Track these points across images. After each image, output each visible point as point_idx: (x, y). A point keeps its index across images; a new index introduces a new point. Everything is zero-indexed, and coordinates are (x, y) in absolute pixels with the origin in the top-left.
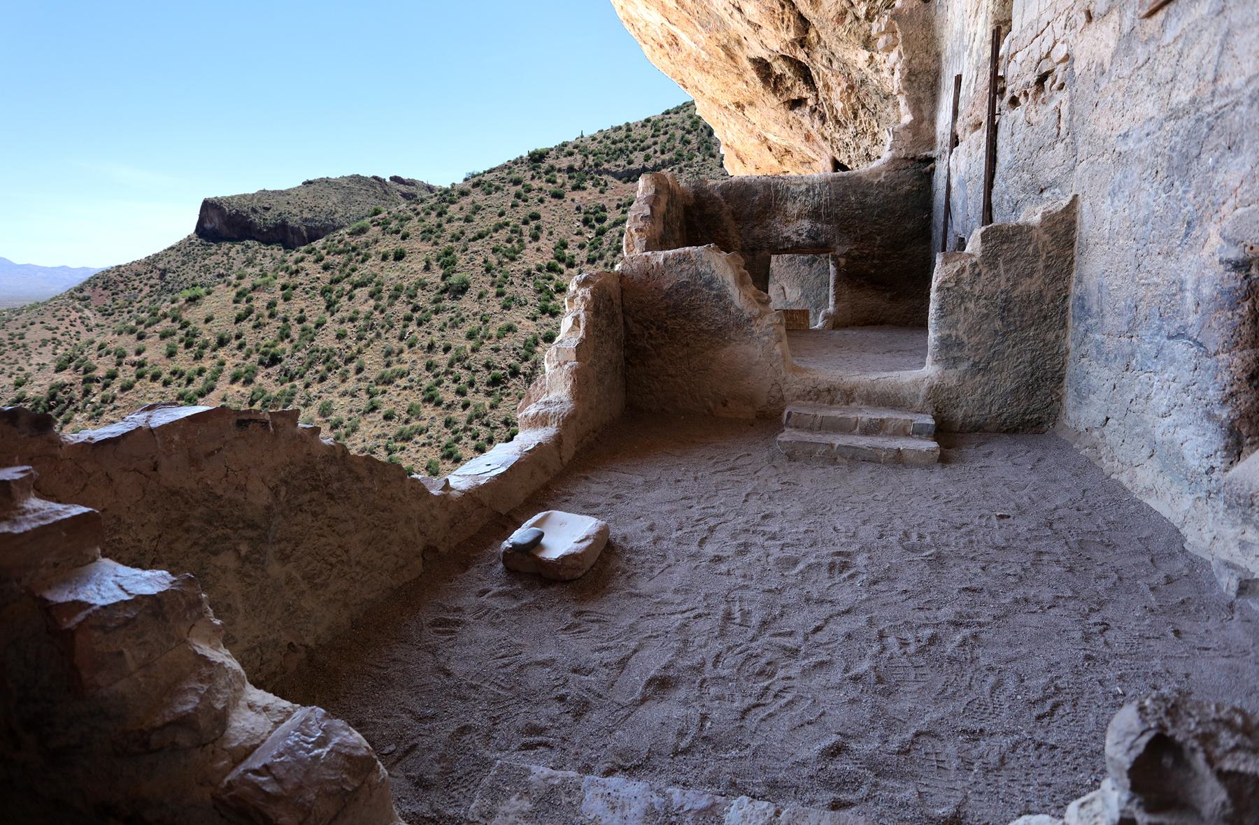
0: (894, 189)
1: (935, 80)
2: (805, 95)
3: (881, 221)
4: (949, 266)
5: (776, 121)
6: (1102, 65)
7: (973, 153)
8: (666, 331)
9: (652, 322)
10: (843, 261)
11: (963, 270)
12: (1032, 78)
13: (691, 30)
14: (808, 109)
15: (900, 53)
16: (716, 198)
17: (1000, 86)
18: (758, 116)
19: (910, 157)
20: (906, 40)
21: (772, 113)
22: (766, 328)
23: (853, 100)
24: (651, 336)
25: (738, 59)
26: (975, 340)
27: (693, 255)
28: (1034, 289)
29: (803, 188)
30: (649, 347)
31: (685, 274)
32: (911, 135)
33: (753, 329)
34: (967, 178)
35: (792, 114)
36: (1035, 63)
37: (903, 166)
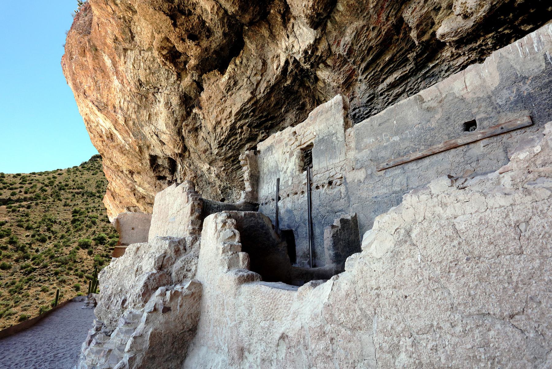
2: (167, 175)
4: (333, 229)
5: (149, 183)
6: (360, 180)
11: (337, 231)
14: (167, 181)
18: (140, 179)
20: (250, 164)
21: (149, 179)
23: (195, 182)
25: (143, 154)
26: (343, 254)
27: (256, 214)
28: (353, 238)
29: (216, 206)
31: (253, 222)
34: (293, 209)
35: (158, 182)
36: (327, 178)
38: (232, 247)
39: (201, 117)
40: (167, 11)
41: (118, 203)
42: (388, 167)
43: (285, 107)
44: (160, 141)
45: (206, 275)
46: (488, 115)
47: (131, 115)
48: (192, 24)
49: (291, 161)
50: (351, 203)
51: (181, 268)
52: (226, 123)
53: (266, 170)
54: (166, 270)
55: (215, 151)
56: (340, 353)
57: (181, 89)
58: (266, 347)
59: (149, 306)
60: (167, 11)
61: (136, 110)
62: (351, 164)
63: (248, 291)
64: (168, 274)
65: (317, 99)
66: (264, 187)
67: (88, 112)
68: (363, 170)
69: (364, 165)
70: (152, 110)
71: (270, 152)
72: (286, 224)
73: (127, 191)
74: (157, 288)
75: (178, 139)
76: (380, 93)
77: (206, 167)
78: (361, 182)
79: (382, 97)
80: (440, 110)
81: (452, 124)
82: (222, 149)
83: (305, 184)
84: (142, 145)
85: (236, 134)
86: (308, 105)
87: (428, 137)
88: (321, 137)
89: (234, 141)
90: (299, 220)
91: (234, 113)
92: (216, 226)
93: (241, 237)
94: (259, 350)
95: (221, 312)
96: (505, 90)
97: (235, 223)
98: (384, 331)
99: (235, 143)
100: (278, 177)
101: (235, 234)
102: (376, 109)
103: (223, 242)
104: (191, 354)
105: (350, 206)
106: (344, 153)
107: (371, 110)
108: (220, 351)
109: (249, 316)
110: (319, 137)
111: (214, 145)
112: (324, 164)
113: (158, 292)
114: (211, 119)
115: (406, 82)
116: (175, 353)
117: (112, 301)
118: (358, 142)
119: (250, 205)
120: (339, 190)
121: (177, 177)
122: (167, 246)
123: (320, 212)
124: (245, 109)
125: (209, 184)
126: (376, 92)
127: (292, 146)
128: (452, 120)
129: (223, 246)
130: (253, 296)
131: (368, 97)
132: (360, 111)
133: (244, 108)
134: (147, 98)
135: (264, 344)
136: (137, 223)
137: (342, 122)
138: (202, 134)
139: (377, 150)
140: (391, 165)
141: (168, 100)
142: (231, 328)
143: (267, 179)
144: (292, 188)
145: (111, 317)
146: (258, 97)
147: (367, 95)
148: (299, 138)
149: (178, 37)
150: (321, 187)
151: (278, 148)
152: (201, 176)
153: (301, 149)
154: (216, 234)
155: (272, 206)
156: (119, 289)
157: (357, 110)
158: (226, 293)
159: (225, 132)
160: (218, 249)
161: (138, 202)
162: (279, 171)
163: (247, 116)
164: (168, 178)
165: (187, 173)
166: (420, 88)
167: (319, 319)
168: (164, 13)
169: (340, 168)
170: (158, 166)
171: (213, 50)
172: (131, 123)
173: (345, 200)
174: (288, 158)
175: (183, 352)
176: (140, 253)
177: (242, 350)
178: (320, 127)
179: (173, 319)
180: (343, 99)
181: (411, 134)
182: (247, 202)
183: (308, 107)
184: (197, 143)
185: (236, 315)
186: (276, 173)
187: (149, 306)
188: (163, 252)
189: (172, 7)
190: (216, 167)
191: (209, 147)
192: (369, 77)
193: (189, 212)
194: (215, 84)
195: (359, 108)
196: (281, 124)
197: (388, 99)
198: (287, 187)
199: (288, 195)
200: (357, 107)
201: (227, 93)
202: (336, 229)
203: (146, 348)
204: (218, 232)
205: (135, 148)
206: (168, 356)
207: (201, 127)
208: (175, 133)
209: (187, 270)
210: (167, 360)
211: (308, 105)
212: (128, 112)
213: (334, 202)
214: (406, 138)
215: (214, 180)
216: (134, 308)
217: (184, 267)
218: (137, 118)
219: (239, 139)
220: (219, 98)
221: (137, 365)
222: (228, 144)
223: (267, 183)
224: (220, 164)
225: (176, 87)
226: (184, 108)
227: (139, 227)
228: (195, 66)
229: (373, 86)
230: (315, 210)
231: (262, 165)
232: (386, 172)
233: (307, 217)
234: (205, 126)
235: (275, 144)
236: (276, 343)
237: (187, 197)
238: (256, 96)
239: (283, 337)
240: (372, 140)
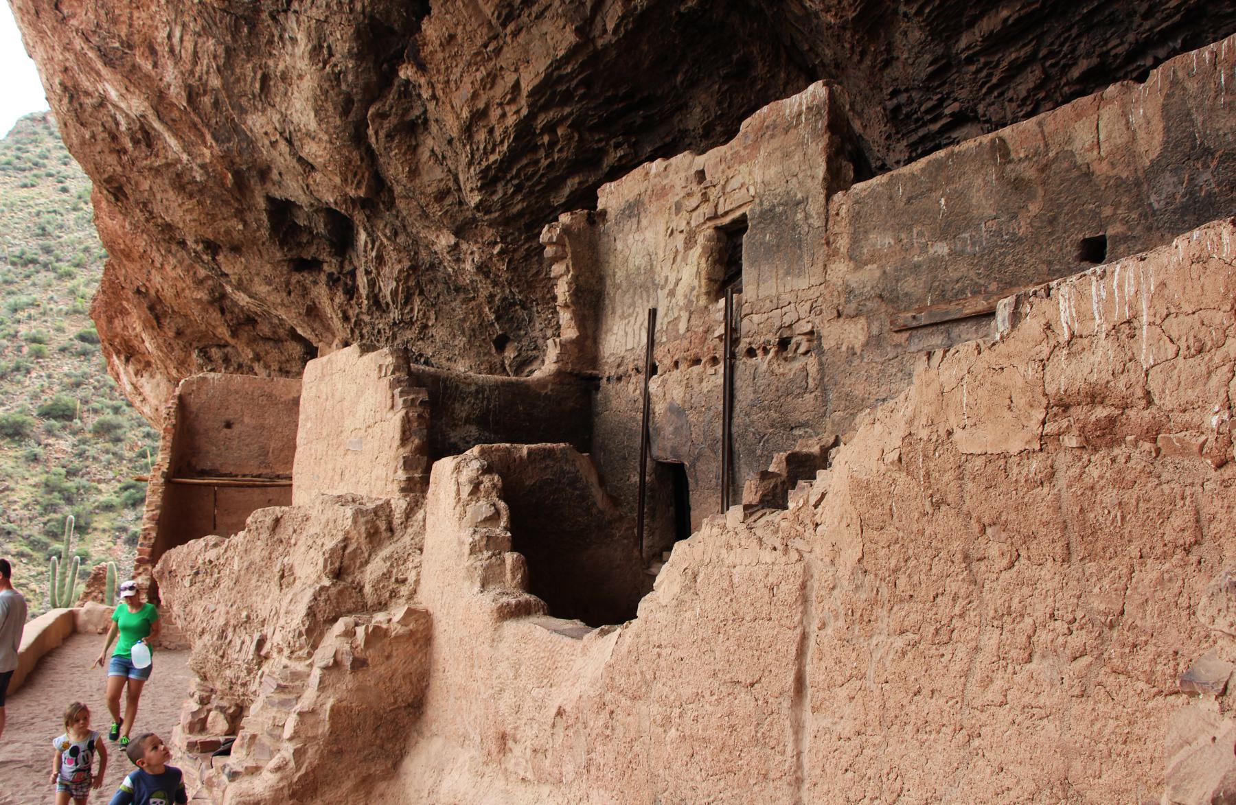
1: (598, 301)
2: (324, 256)
4: (765, 483)
6: (853, 348)
7: (696, 385)
11: (776, 486)
12: (774, 339)
14: (323, 278)
15: (567, 267)
17: (734, 336)
21: (268, 270)
22: (626, 530)
23: (412, 283)
29: (473, 388)
31: (549, 470)
32: (576, 350)
33: (613, 531)
34: (687, 406)
35: (296, 277)
36: (775, 328)
38: (491, 542)
39: (426, 94)
41: (171, 334)
42: (914, 324)
43: (687, 71)
44: (300, 160)
45: (439, 596)
46: (1129, 229)
47: (205, 77)
49: (689, 261)
50: (831, 407)
51: (384, 574)
52: (504, 115)
53: (620, 275)
54: (350, 580)
55: (474, 199)
56: (620, 731)
58: (539, 730)
59: (324, 655)
61: (221, 61)
62: (836, 301)
63: (515, 635)
64: (355, 588)
66: (615, 328)
67: (71, 63)
68: (863, 320)
69: (865, 309)
70: (271, 63)
71: (635, 220)
72: (668, 444)
74: (335, 620)
75: (356, 156)
76: (963, 56)
77: (445, 240)
78: (854, 354)
79: (973, 68)
80: (1041, 192)
81: (1058, 238)
83: (720, 337)
84: (244, 167)
85: (536, 148)
86: (760, 64)
87: (1009, 259)
88: (766, 205)
90: (701, 438)
91: (526, 87)
92: (458, 490)
93: (513, 519)
94: (528, 735)
95: (468, 670)
96: (1168, 174)
97: (500, 484)
98: (663, 700)
99: (535, 173)
100: (650, 306)
101: (497, 512)
102: (955, 100)
103: (471, 530)
104: (413, 752)
105: (828, 415)
106: (821, 265)
107: (941, 102)
108: (467, 742)
109: (516, 679)
110: (761, 203)
111: (469, 180)
112: (770, 288)
113: (340, 626)
114: (457, 103)
115: (1039, 31)
116: (382, 747)
117: (231, 641)
118: (855, 241)
120: (804, 369)
121: (356, 263)
122: (350, 522)
123: (753, 422)
124: (561, 78)
125: (457, 290)
126: (954, 51)
127: (695, 214)
128: (1061, 225)
129: (471, 540)
130: (523, 645)
131: (930, 65)
132: (910, 101)
133: (555, 74)
134: (253, 27)
135: (536, 726)
136: (239, 407)
137: (821, 171)
138: (430, 142)
139: (896, 270)
140: (923, 322)
141: (320, 38)
142: (485, 700)
143: (623, 303)
144: (685, 343)
145: (232, 676)
146: (600, 43)
147: (928, 57)
148: (713, 193)
150: (760, 352)
151: (656, 214)
152: (432, 266)
153: (717, 228)
154: (458, 508)
155: (632, 389)
156: (244, 614)
157: (903, 98)
158: (478, 635)
159: (502, 142)
160: (461, 543)
161: (234, 334)
162: (657, 287)
163: (567, 98)
164: (325, 267)
165: (386, 258)
166: (1077, 53)
167: (598, 685)
169: (807, 306)
170: (295, 229)
172: (207, 100)
173: (816, 398)
174: (681, 247)
175: (397, 747)
176: (285, 532)
177: (503, 737)
178: (767, 173)
179: (372, 682)
180: (831, 96)
181: (974, 244)
182: (565, 373)
183: (760, 69)
184: (414, 173)
185: (494, 677)
186: (647, 289)
187: (324, 655)
188: (340, 537)
190: (476, 242)
191: (451, 184)
192: (927, 11)
193: (398, 436)
195: (907, 90)
196: (676, 120)
197: (990, 76)
198: (676, 338)
199: (676, 365)
200: (903, 88)
201: (504, 25)
202: (773, 482)
203: (323, 735)
204: (461, 504)
206: (366, 752)
207: (426, 121)
209: (397, 580)
210: (365, 760)
211: (760, 64)
212: (198, 68)
213: (789, 399)
214: (961, 253)
215: (472, 281)
216: (290, 658)
217: (390, 572)
218: (226, 86)
219: (544, 163)
220: (479, 42)
221: (311, 763)
222: (512, 178)
223: (623, 317)
224: (489, 234)
226: (371, 65)
227: (246, 420)
229: (945, 35)
230: (741, 415)
231: (612, 259)
232: (911, 335)
233: (719, 433)
234: (437, 121)
235: (646, 200)
236: (550, 723)
237: (389, 395)
238: (593, 40)
239: (560, 713)
240: (889, 240)
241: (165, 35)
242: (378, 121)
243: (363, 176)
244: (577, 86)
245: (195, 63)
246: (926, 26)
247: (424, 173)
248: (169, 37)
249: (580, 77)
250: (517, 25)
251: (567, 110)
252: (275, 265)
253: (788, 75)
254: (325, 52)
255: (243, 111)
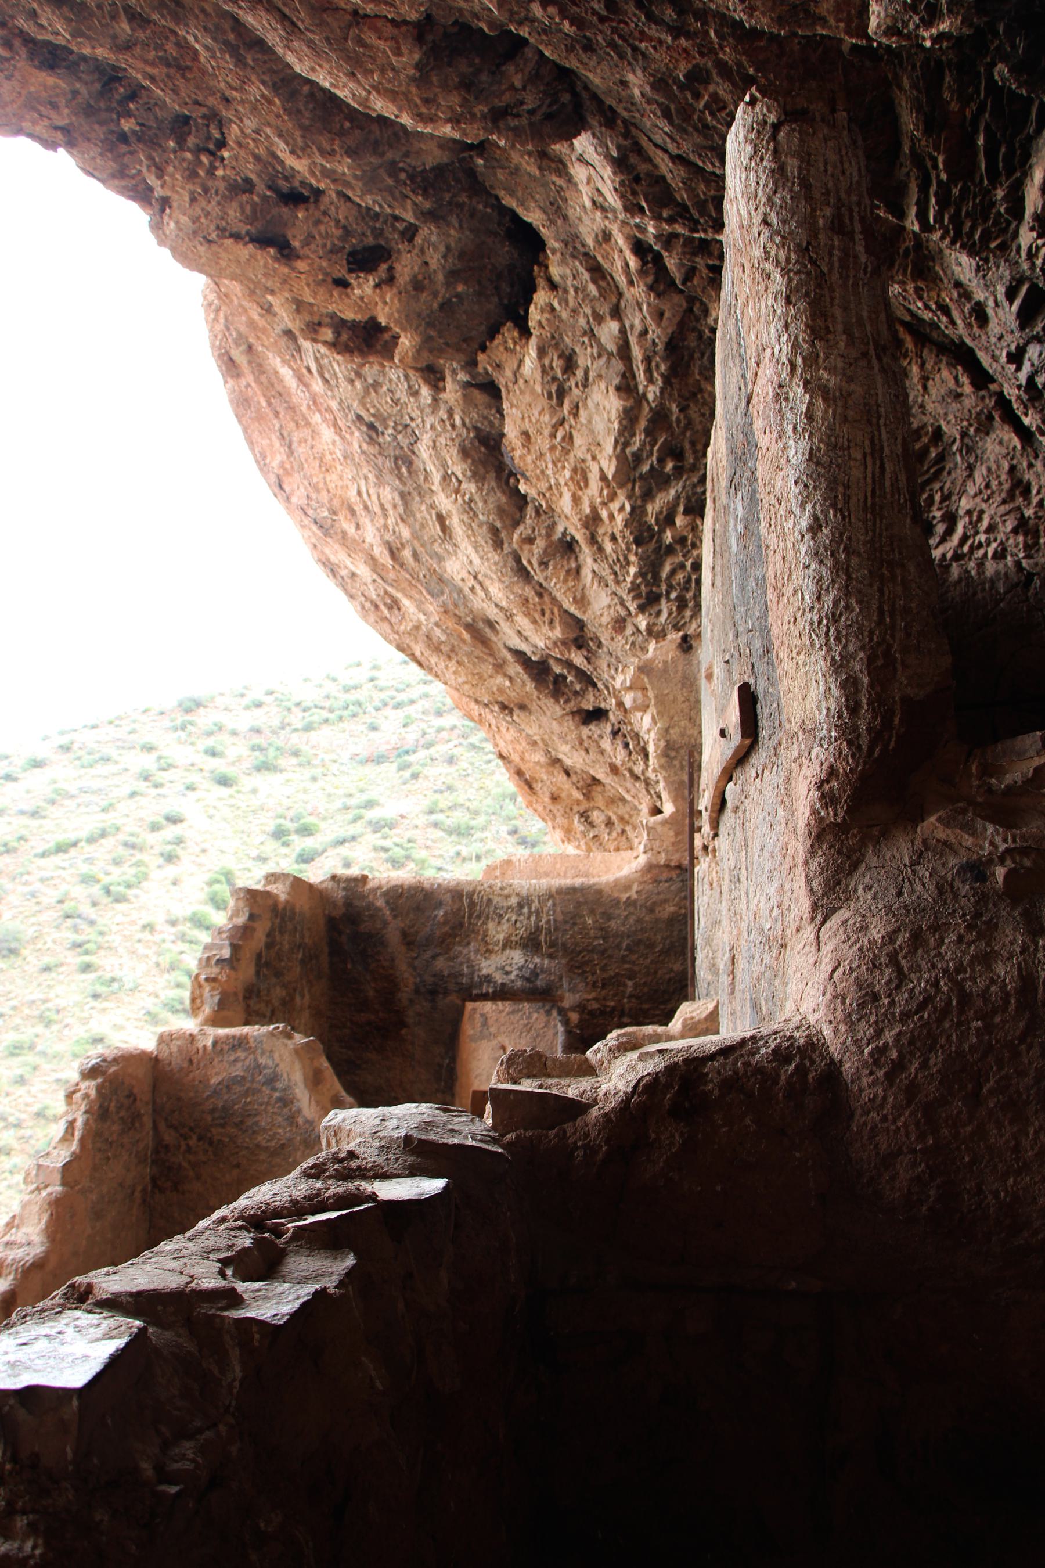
0: (651, 910)
3: (634, 957)
8: (211, 1143)
9: (192, 1129)
10: (574, 1017)
13: (414, 593)
14: (609, 728)
15: (653, 718)
16: (379, 909)
19: (673, 864)
20: (660, 700)
24: (189, 1149)
27: (251, 1040)
29: (514, 901)
30: (185, 1164)
32: (672, 833)
35: (585, 731)
37: (665, 876)
40: (244, 228)
41: (547, 799)
48: (338, 222)
52: (612, 517)
55: (642, 622)
57: (458, 421)
60: (244, 228)
61: (401, 509)
65: (908, 318)
73: (538, 763)
75: (529, 592)
82: (659, 613)
89: (680, 576)
119: (674, 874)
149: (320, 283)
159: (629, 550)
168: (236, 237)
171: (440, 277)
172: (407, 553)
182: (658, 866)
189: (254, 205)
191: (619, 608)
194: (521, 382)
201: (561, 404)
205: (459, 636)
208: (510, 573)
212: (389, 521)
220: (546, 432)
225: (445, 417)
226: (493, 484)
228: (418, 351)
241: (355, 493)
242: (526, 547)
243: (552, 613)
244: (661, 461)
245: (386, 516)
246: (953, 243)
247: (592, 600)
248: (359, 493)
249: (656, 448)
250: (571, 402)
251: (672, 492)
252: (560, 720)
253: (922, 366)
254: (454, 479)
255: (440, 559)
